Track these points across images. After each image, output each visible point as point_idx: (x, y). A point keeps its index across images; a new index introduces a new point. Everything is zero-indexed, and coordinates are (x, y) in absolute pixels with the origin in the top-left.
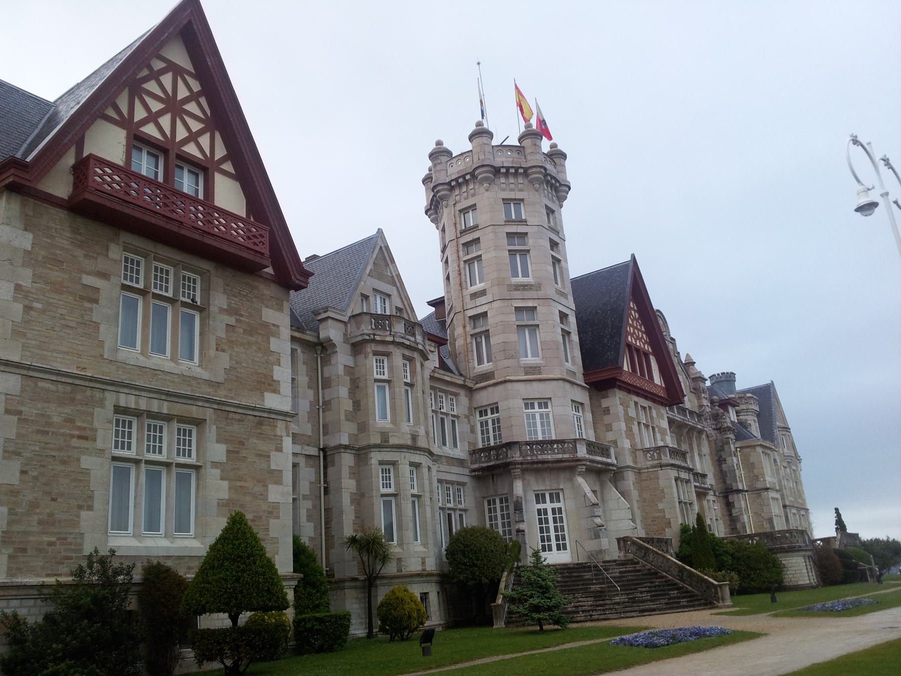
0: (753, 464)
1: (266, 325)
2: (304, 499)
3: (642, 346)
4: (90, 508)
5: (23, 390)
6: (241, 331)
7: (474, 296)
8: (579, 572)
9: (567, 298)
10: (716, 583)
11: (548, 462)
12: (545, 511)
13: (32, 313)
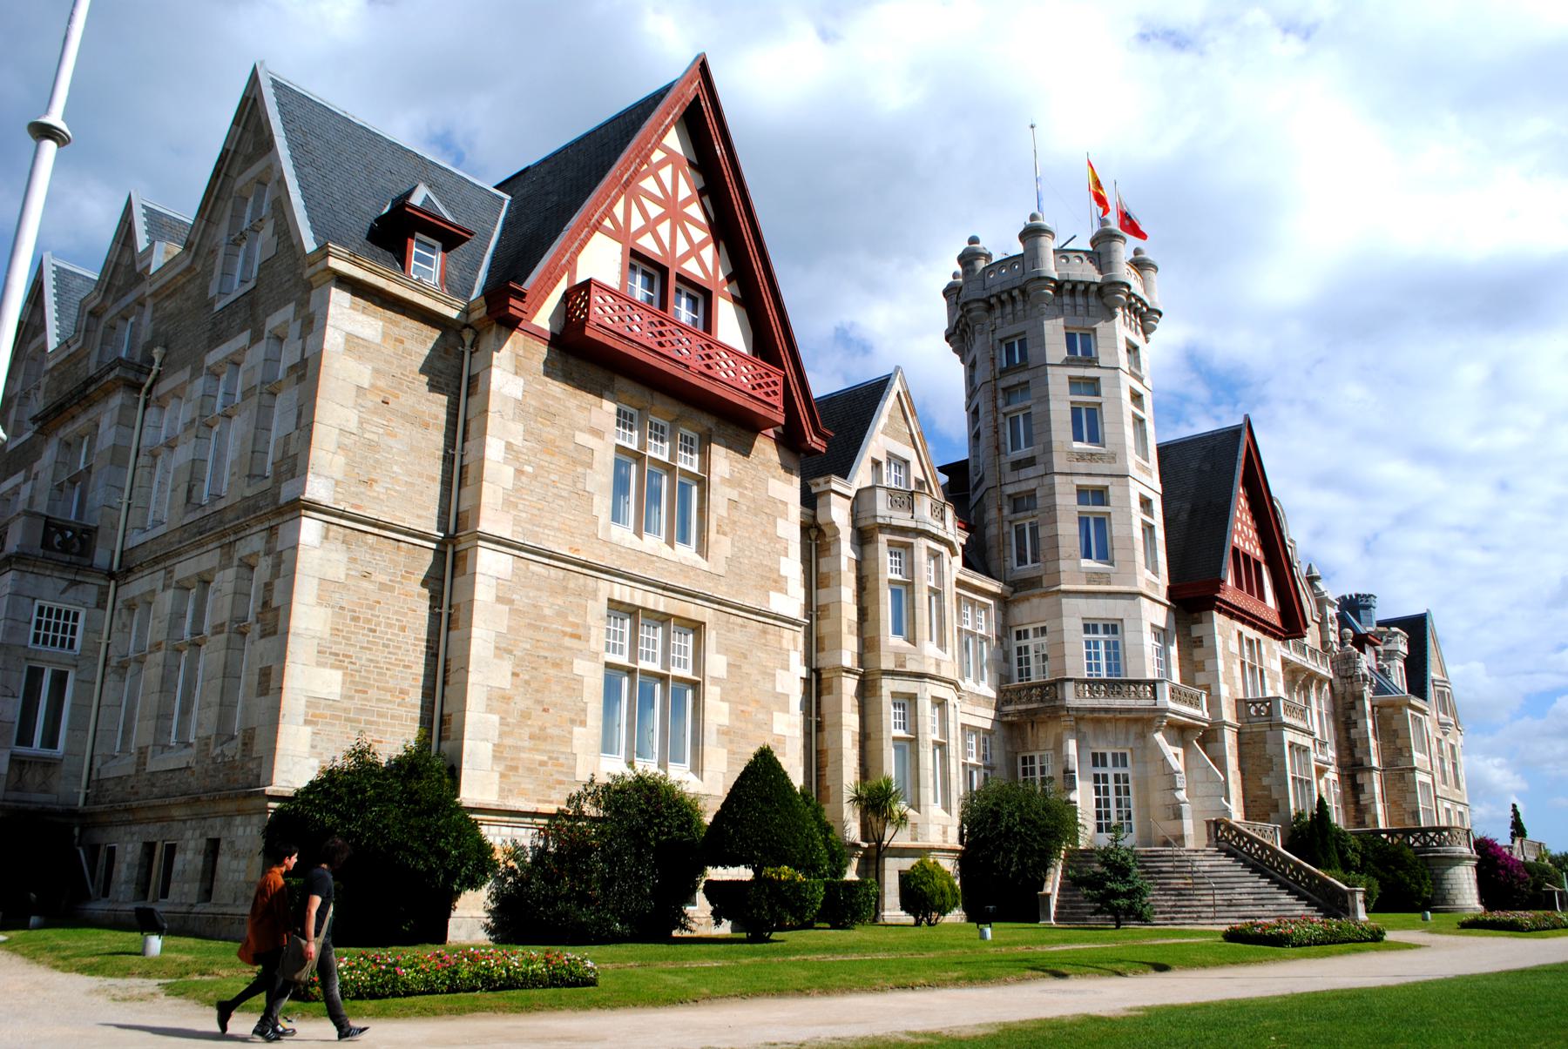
0: (1395, 731)
1: (773, 501)
3: (1253, 550)
4: (583, 723)
5: (514, 573)
6: (745, 508)
7: (1018, 465)
8: (1154, 862)
9: (1151, 476)
10: (1346, 888)
11: (1115, 710)
12: (1105, 777)
13: (524, 479)
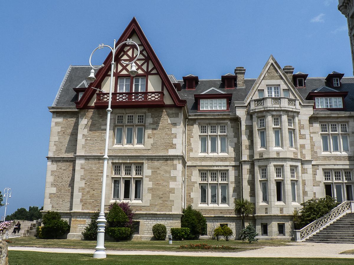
2: (231, 183)
